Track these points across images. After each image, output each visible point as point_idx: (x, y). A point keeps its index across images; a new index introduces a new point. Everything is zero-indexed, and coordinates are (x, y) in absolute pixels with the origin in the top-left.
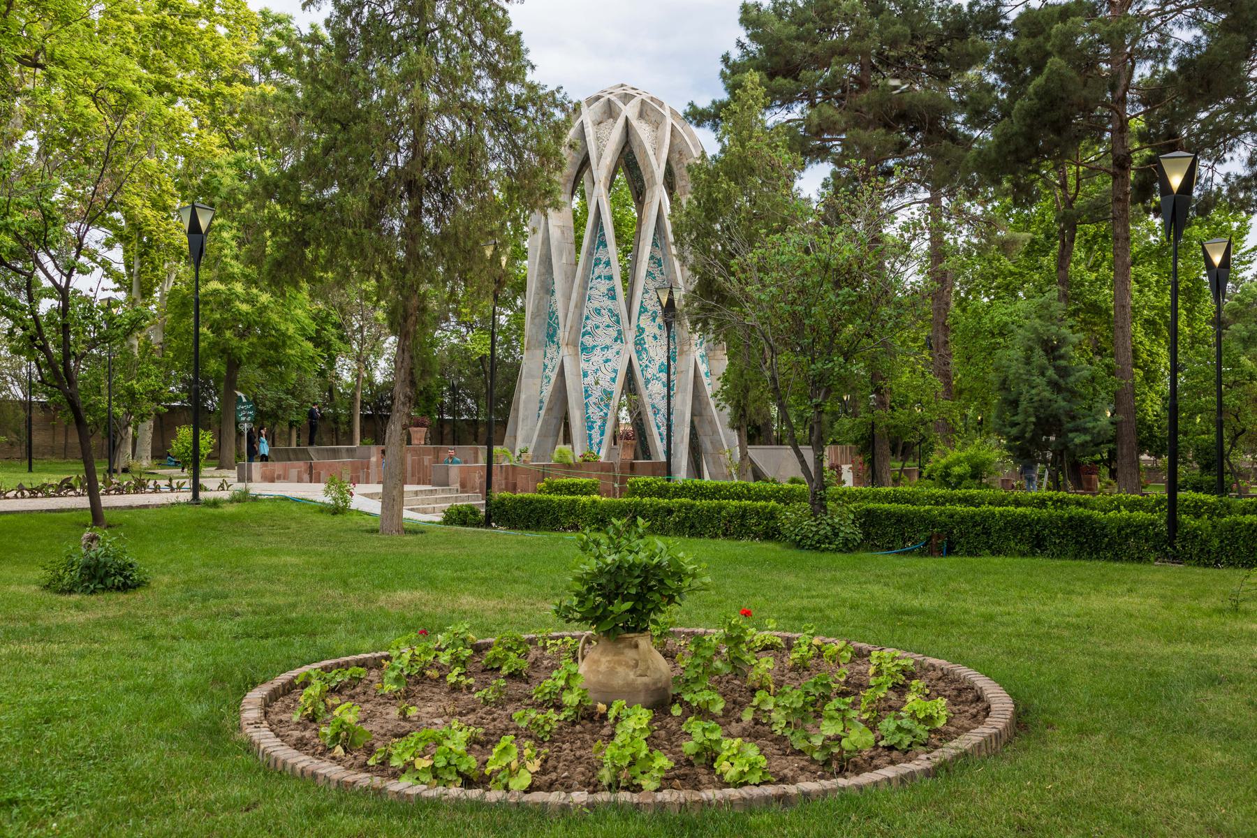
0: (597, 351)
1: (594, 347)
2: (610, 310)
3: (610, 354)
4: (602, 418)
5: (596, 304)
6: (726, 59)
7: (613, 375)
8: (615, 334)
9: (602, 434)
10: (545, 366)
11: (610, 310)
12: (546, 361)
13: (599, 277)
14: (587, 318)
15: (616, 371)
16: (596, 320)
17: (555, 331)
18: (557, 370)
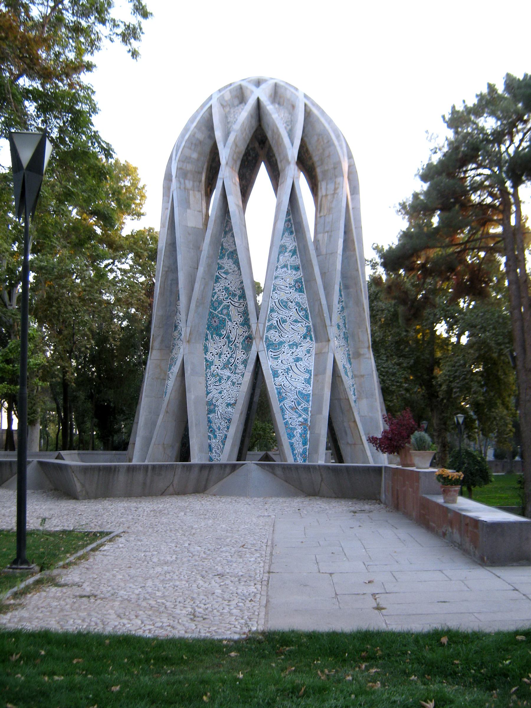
0: (286, 348)
1: (281, 343)
2: (298, 304)
3: (300, 352)
4: (302, 424)
5: (283, 296)
6: (454, 107)
7: (307, 376)
8: (304, 330)
9: (292, 445)
10: (209, 364)
11: (298, 304)
12: (209, 356)
13: (285, 266)
14: (272, 310)
15: (309, 372)
16: (284, 313)
17: (223, 323)
18: (251, 367)
